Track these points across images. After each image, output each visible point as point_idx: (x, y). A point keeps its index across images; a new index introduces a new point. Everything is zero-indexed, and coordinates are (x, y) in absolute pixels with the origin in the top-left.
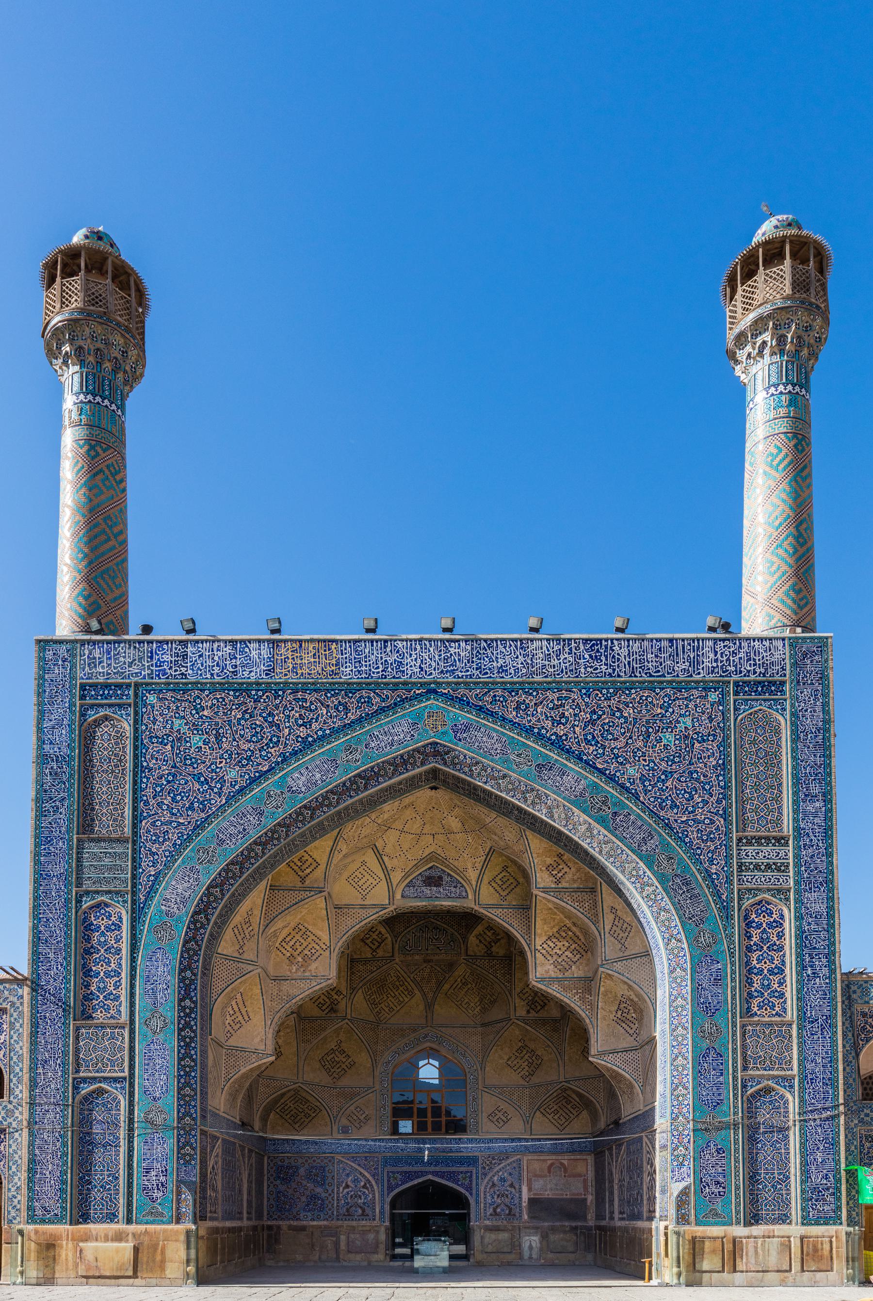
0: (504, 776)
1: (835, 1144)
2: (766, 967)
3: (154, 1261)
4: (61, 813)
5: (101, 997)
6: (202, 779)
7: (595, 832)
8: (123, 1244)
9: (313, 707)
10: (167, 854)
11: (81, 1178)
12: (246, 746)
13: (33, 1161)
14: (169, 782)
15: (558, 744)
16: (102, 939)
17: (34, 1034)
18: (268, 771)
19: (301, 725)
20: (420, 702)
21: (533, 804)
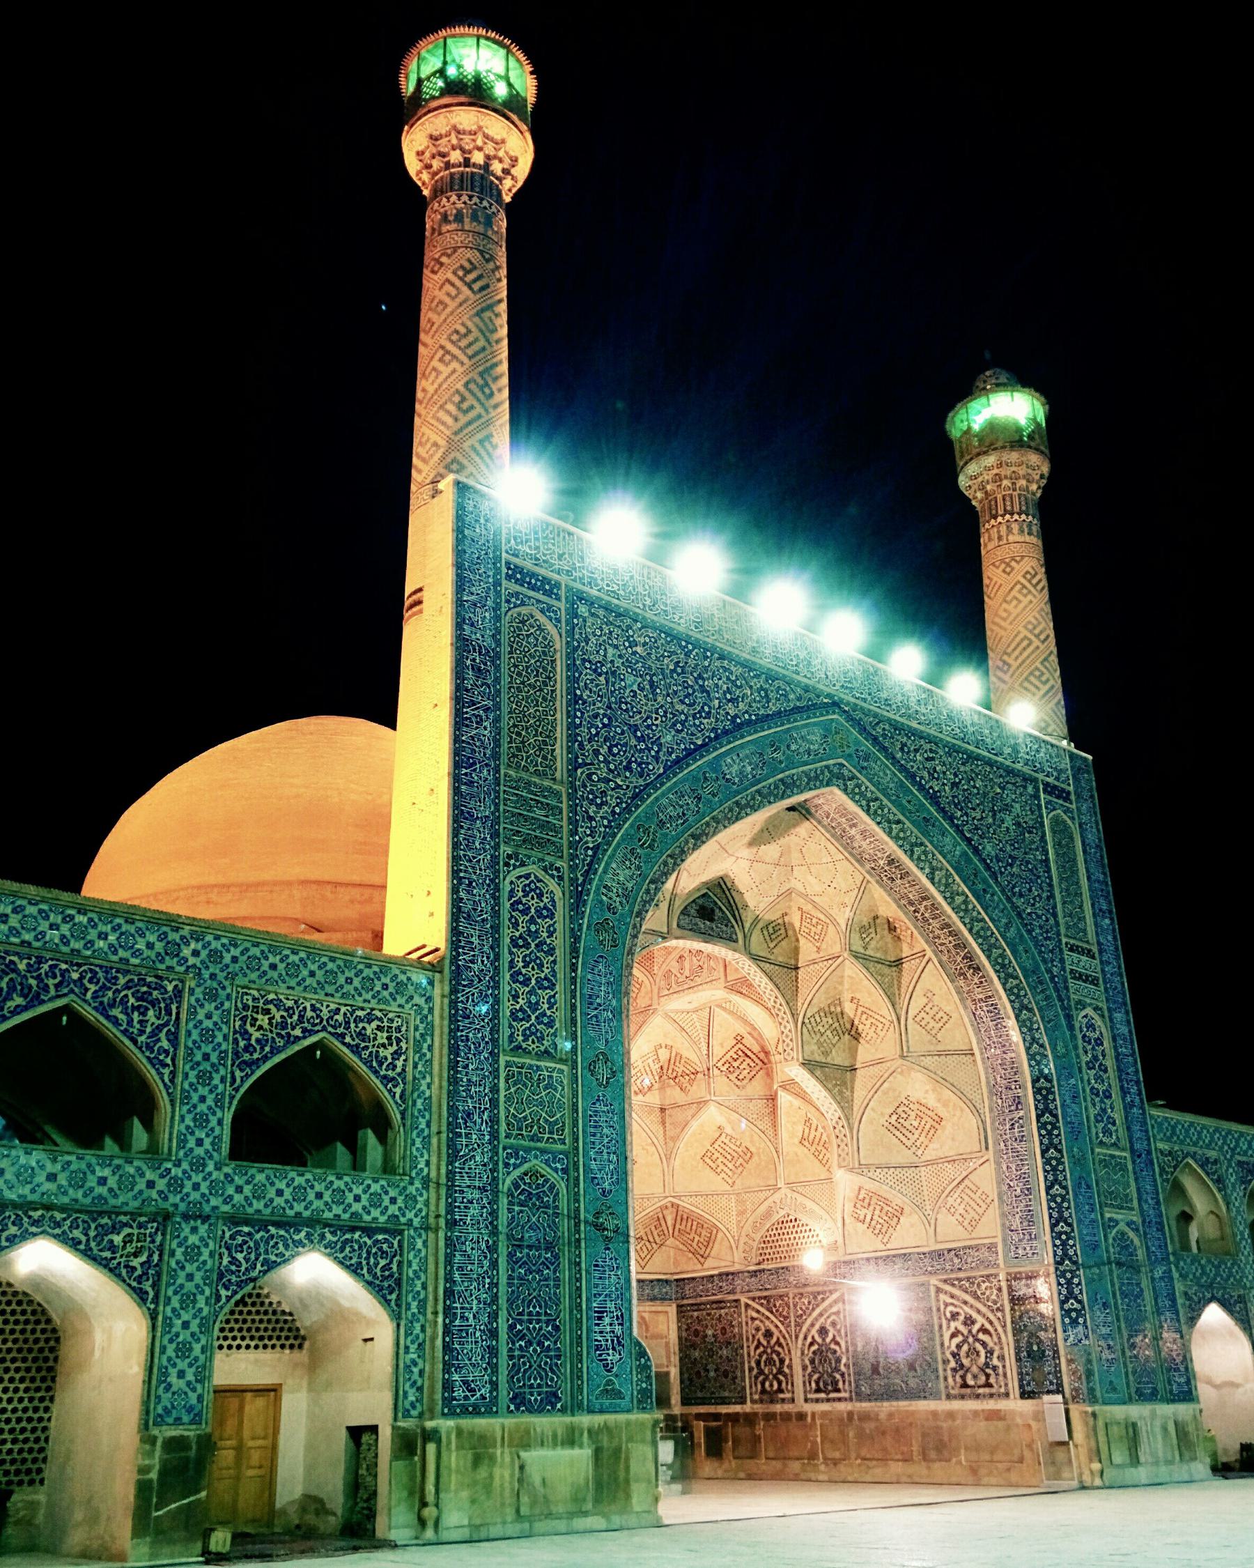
0: (898, 822)
1: (1174, 1301)
2: (1101, 1088)
3: (616, 1479)
4: (485, 728)
5: (533, 1017)
6: (639, 734)
7: (970, 907)
8: (576, 1452)
9: (738, 683)
10: (605, 822)
11: (512, 1327)
12: (680, 707)
13: (449, 1293)
14: (604, 726)
15: (934, 798)
16: (533, 928)
17: (453, 1065)
18: (702, 746)
19: (729, 701)
20: (828, 713)
21: (919, 858)
